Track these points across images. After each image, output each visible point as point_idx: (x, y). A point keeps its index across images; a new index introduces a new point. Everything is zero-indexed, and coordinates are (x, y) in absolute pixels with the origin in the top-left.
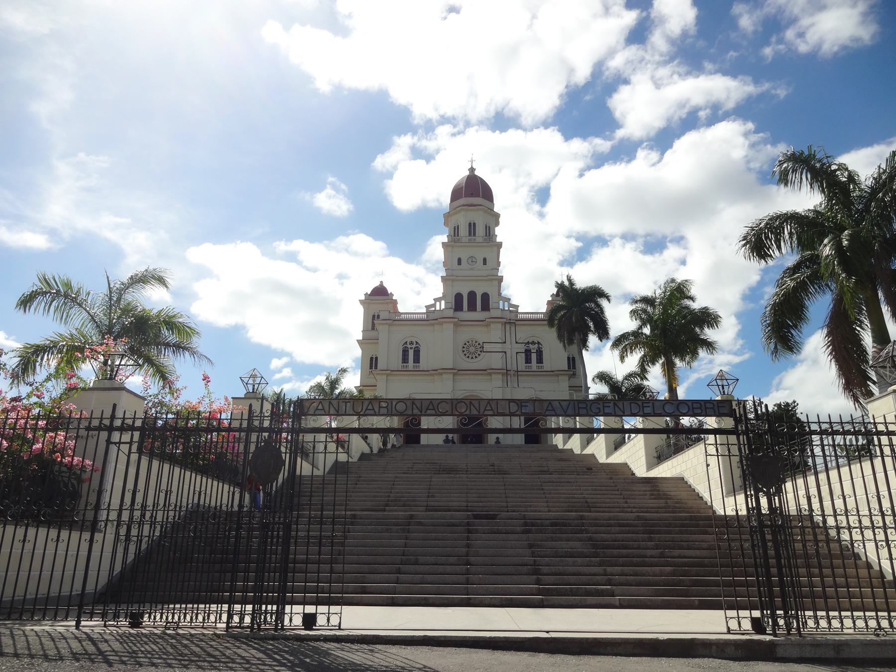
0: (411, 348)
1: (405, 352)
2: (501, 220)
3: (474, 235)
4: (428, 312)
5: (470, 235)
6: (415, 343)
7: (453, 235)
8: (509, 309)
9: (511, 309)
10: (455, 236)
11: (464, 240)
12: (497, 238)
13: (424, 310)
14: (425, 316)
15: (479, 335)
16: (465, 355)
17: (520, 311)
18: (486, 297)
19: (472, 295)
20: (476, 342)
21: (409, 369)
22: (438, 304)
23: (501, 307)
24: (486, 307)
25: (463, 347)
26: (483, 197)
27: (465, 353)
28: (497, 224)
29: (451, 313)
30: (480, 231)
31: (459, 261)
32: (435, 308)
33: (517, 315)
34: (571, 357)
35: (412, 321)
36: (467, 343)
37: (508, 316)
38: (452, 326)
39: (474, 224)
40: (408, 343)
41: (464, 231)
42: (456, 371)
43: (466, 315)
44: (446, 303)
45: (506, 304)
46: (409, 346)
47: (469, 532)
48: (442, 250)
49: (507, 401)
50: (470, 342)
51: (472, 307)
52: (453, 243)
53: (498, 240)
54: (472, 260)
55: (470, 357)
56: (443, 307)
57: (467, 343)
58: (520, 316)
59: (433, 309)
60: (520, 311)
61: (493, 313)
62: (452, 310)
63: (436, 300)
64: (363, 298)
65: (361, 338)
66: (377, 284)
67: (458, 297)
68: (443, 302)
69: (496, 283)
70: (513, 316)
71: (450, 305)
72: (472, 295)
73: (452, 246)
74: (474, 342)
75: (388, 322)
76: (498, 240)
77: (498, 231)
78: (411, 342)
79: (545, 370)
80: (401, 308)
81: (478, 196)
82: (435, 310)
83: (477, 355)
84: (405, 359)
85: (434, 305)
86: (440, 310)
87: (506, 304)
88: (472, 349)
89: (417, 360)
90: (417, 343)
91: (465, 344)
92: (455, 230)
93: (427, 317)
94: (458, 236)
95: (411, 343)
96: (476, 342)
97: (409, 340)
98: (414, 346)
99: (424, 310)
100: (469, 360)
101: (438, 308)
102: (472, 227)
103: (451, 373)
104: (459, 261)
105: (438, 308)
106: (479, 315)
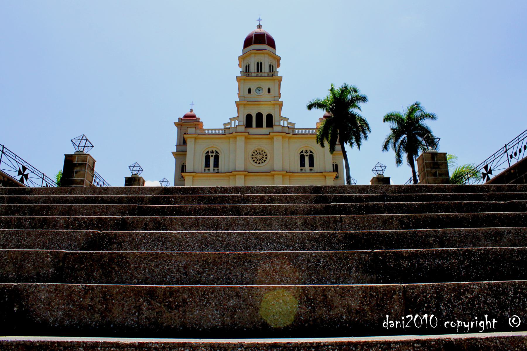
0: (212, 156)
1: (207, 158)
3: (261, 71)
4: (225, 129)
5: (258, 71)
6: (215, 152)
7: (245, 72)
8: (287, 125)
9: (289, 126)
10: (246, 72)
11: (253, 75)
14: (223, 132)
15: (263, 145)
16: (254, 161)
18: (270, 117)
19: (259, 116)
20: (262, 151)
21: (210, 172)
22: (233, 122)
23: (282, 124)
24: (270, 124)
25: (252, 155)
26: (267, 44)
27: (253, 159)
28: (279, 65)
29: (243, 128)
30: (266, 69)
31: (250, 91)
32: (231, 125)
34: (335, 164)
35: (214, 135)
36: (256, 152)
37: (287, 130)
38: (243, 138)
39: (261, 63)
40: (210, 152)
41: (253, 68)
42: (247, 173)
43: (254, 130)
44: (239, 121)
45: (285, 122)
46: (210, 154)
50: (258, 151)
51: (259, 125)
52: (245, 77)
53: (279, 75)
54: (259, 89)
56: (237, 124)
58: (296, 132)
59: (230, 126)
61: (276, 128)
62: (244, 127)
66: (187, 112)
67: (249, 117)
68: (237, 122)
69: (278, 106)
70: (291, 131)
71: (242, 123)
72: (259, 116)
74: (261, 151)
78: (212, 151)
79: (315, 172)
80: (204, 127)
81: (264, 43)
84: (207, 165)
86: (235, 127)
87: (285, 122)
88: (259, 157)
89: (216, 165)
90: (217, 152)
91: (254, 153)
94: (249, 72)
95: (212, 152)
96: (262, 151)
97: (210, 150)
98: (214, 154)
100: (257, 165)
101: (233, 126)
102: (260, 67)
103: (243, 174)
104: (250, 91)
105: (233, 126)
106: (264, 130)
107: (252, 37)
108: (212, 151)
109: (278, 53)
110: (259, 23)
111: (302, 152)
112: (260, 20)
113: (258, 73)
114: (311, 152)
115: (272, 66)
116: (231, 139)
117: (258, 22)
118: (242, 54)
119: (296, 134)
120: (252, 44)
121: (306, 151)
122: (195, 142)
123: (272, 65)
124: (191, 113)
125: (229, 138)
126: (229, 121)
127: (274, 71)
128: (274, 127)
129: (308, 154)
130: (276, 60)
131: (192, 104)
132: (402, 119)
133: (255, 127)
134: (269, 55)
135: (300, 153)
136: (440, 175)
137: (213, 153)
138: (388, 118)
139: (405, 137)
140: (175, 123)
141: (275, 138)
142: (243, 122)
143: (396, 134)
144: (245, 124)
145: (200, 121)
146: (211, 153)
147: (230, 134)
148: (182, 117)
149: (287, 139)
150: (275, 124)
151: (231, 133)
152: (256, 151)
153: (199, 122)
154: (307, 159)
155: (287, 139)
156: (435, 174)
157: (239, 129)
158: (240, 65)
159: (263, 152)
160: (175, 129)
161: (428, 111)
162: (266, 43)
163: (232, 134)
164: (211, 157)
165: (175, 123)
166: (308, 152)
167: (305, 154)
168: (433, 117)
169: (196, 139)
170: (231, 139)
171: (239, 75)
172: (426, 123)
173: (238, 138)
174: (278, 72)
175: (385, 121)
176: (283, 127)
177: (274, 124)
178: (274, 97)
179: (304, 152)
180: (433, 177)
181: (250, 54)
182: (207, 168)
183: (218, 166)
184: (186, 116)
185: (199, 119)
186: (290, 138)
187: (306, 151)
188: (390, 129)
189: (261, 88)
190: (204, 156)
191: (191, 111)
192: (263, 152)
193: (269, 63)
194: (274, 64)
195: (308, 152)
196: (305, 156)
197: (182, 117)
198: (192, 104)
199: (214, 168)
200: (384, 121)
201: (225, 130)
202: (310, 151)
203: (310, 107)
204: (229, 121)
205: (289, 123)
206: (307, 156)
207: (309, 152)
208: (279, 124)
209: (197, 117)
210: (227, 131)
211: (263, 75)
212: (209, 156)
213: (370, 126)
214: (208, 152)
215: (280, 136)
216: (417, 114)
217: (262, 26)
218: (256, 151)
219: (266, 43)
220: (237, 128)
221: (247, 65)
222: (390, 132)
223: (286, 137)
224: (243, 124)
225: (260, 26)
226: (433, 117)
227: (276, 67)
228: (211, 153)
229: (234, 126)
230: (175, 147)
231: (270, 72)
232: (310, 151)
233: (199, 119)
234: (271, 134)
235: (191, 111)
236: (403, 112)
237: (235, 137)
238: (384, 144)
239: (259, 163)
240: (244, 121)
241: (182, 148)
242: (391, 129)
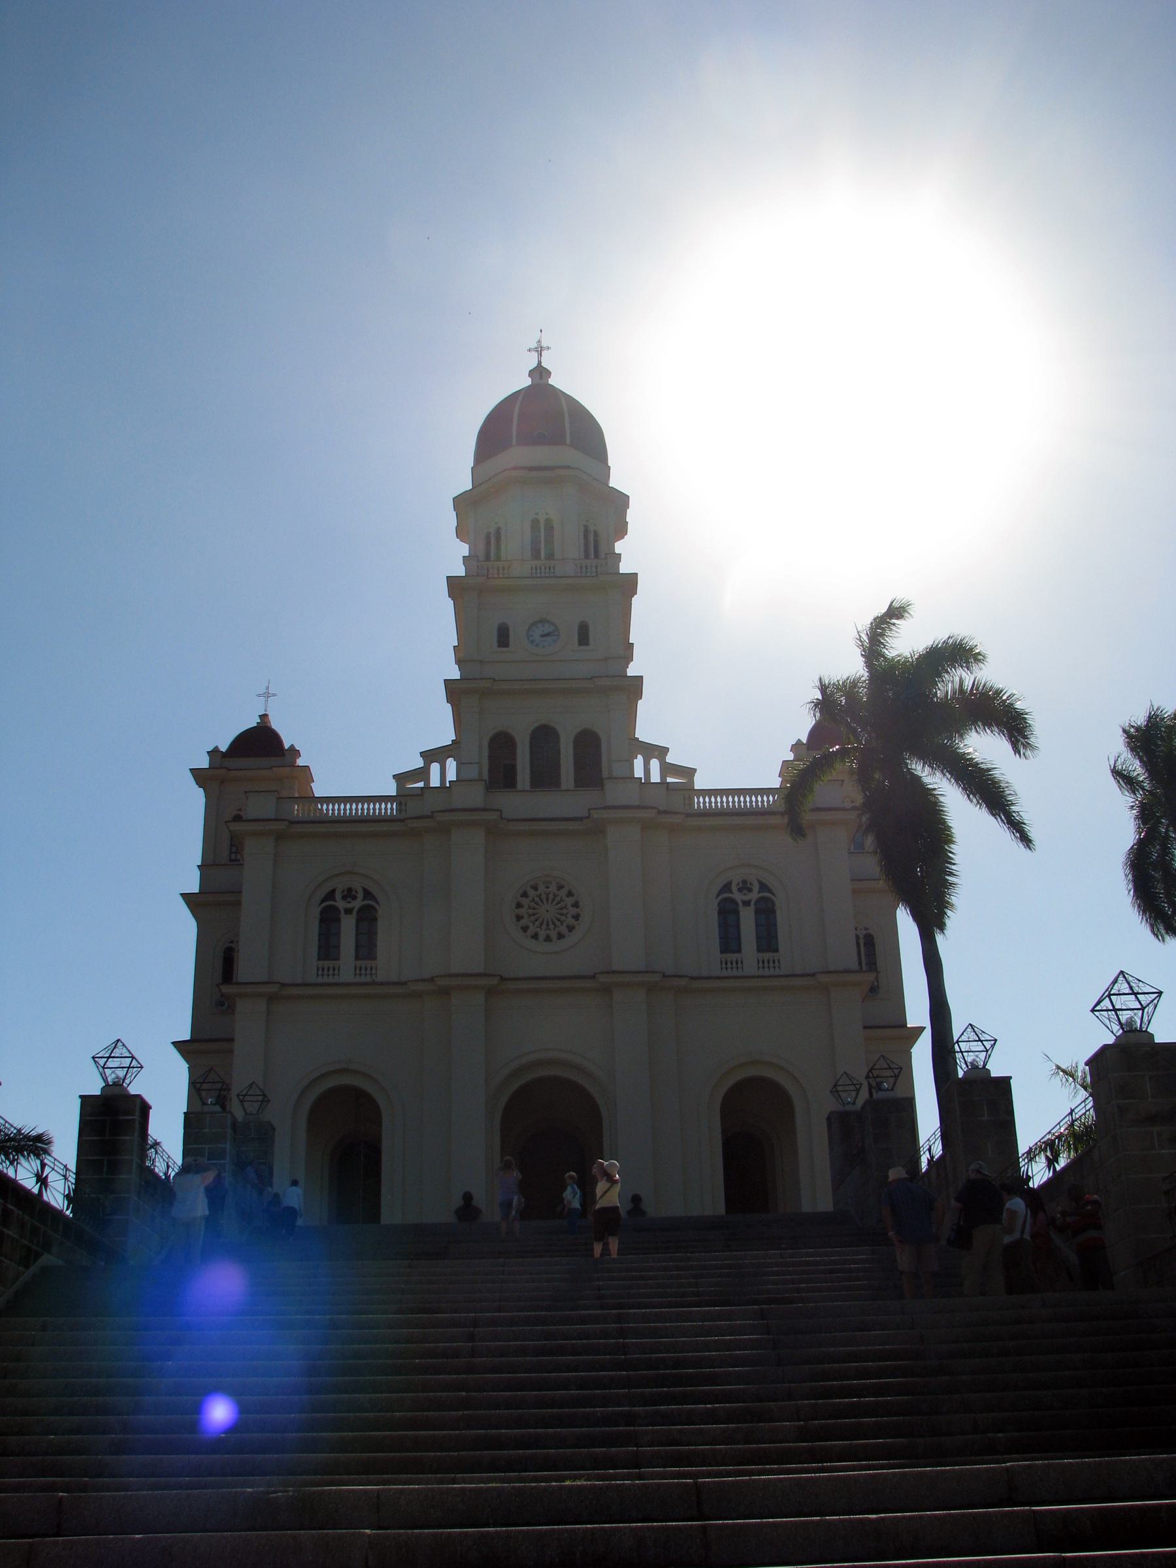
0: (348, 911)
4: (402, 797)
6: (360, 895)
8: (663, 775)
9: (669, 780)
13: (391, 789)
14: (390, 809)
17: (700, 783)
19: (544, 736)
20: (560, 887)
21: (342, 979)
22: (435, 768)
23: (639, 772)
25: (519, 905)
27: (523, 922)
29: (475, 796)
32: (427, 781)
33: (691, 800)
34: (861, 934)
36: (531, 893)
40: (338, 896)
42: (495, 981)
48: (450, 603)
50: (542, 888)
53: (624, 568)
55: (541, 938)
56: (451, 775)
57: (531, 893)
58: (700, 802)
59: (421, 784)
60: (698, 785)
63: (430, 756)
64: (204, 763)
67: (501, 745)
68: (451, 764)
71: (473, 772)
74: (553, 888)
75: (274, 826)
78: (350, 890)
80: (320, 789)
83: (563, 929)
85: (423, 773)
87: (655, 764)
90: (368, 894)
91: (525, 895)
92: (488, 543)
93: (399, 810)
95: (349, 894)
96: (560, 887)
99: (391, 789)
101: (435, 781)
104: (503, 637)
105: (435, 781)
108: (350, 890)
110: (540, 363)
111: (727, 887)
112: (540, 350)
114: (763, 887)
115: (596, 535)
118: (471, 487)
121: (744, 882)
126: (419, 763)
127: (602, 555)
129: (754, 896)
131: (267, 695)
133: (527, 787)
135: (718, 896)
137: (355, 898)
140: (194, 772)
144: (486, 776)
145: (300, 762)
146: (344, 898)
152: (535, 888)
153: (293, 765)
154: (748, 920)
158: (461, 533)
159: (563, 892)
160: (197, 798)
164: (343, 916)
165: (194, 772)
166: (750, 890)
167: (738, 897)
171: (460, 571)
177: (605, 774)
178: (606, 659)
179: (734, 888)
182: (326, 964)
183: (371, 956)
187: (744, 882)
189: (548, 622)
190: (316, 912)
192: (563, 892)
195: (750, 890)
196: (741, 907)
198: (267, 695)
199: (359, 963)
202: (760, 882)
204: (419, 763)
205: (667, 769)
206: (747, 903)
207: (756, 888)
212: (336, 910)
214: (331, 895)
218: (535, 888)
219: (568, 442)
228: (344, 898)
230: (197, 873)
231: (587, 556)
232: (760, 882)
239: (548, 939)
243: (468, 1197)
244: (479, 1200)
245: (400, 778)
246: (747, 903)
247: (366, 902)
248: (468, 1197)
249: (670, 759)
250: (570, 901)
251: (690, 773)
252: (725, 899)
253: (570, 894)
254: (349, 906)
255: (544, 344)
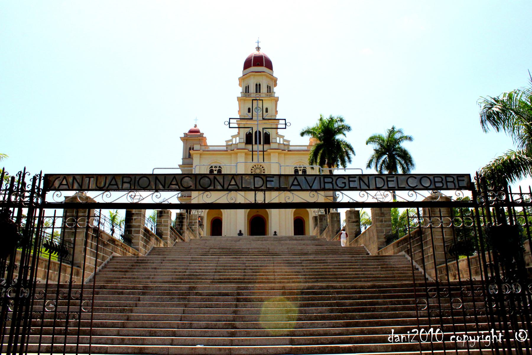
2: (278, 82)
3: (260, 92)
4: (227, 146)
5: (256, 92)
6: (218, 167)
7: (245, 92)
8: (283, 142)
9: (285, 143)
10: (246, 93)
12: (275, 94)
13: (225, 144)
14: (225, 148)
22: (234, 139)
23: (278, 142)
25: (252, 170)
26: (265, 67)
28: (276, 85)
29: (243, 146)
30: (264, 89)
32: (232, 142)
35: (216, 152)
36: (255, 167)
37: (282, 147)
38: (243, 155)
39: (260, 85)
40: (213, 167)
41: (252, 89)
44: (240, 139)
47: (238, 300)
49: (252, 177)
50: (257, 166)
52: (245, 98)
53: (276, 95)
56: (238, 141)
58: (291, 148)
59: (231, 143)
61: (273, 146)
62: (244, 144)
63: (233, 137)
64: (183, 136)
65: (181, 164)
66: (192, 127)
68: (238, 138)
70: (286, 148)
73: (244, 100)
74: (259, 166)
76: (276, 95)
77: (276, 89)
80: (209, 143)
81: (263, 66)
82: (232, 144)
85: (231, 140)
86: (236, 144)
87: (281, 139)
90: (220, 167)
93: (227, 149)
94: (248, 92)
95: (216, 167)
96: (261, 166)
98: (217, 169)
102: (258, 87)
105: (234, 142)
107: (252, 59)
109: (275, 75)
112: (258, 43)
113: (257, 94)
116: (233, 156)
117: (257, 44)
118: (242, 75)
119: (290, 151)
120: (251, 66)
122: (200, 157)
123: (269, 86)
124: (195, 128)
125: (231, 154)
126: (231, 138)
127: (271, 92)
128: (271, 144)
130: (273, 81)
131: (196, 120)
132: (383, 141)
134: (267, 76)
136: (385, 221)
137: (217, 167)
138: (372, 139)
139: (386, 157)
140: (181, 138)
141: (272, 154)
142: (243, 139)
143: (379, 154)
144: (245, 142)
145: (204, 136)
146: (215, 167)
147: (231, 150)
148: (187, 132)
149: (283, 156)
150: (272, 141)
151: (233, 149)
152: (255, 166)
155: (283, 156)
156: (381, 221)
157: (240, 146)
158: (240, 85)
159: (261, 167)
161: (406, 134)
162: (264, 65)
163: (233, 150)
165: (181, 138)
168: (410, 139)
169: (201, 154)
170: (233, 156)
171: (240, 95)
172: (404, 145)
173: (239, 154)
174: (275, 93)
175: (368, 144)
176: (279, 144)
177: (271, 142)
178: (271, 116)
180: (380, 223)
181: (249, 76)
184: (191, 131)
185: (203, 134)
186: (285, 154)
188: (373, 150)
191: (196, 126)
192: (261, 167)
193: (267, 84)
194: (271, 84)
196: (299, 171)
197: (187, 132)
198: (196, 120)
200: (367, 144)
201: (227, 146)
203: (302, 134)
205: (284, 140)
206: (300, 170)
208: (276, 142)
209: (201, 132)
210: (229, 147)
211: (262, 95)
213: (355, 149)
214: (212, 167)
215: (277, 152)
216: (397, 136)
217: (260, 48)
218: (255, 166)
219: (264, 65)
220: (238, 144)
221: (247, 86)
222: (373, 153)
223: (283, 153)
224: (243, 141)
225: (258, 48)
226: (410, 139)
227: (273, 85)
228: (215, 167)
229: (235, 143)
230: (182, 160)
231: (268, 92)
233: (203, 134)
234: (268, 150)
235: (196, 126)
236: (385, 135)
237: (237, 153)
238: (368, 162)
240: (244, 139)
241: (188, 161)
242: (374, 150)
243: (240, 231)
244: (243, 232)
245: (227, 141)
246: (300, 170)
247: (219, 168)
248: (240, 231)
249: (285, 138)
250: (263, 169)
251: (289, 141)
252: (296, 169)
253: (263, 167)
254: (216, 169)
255: (259, 41)
